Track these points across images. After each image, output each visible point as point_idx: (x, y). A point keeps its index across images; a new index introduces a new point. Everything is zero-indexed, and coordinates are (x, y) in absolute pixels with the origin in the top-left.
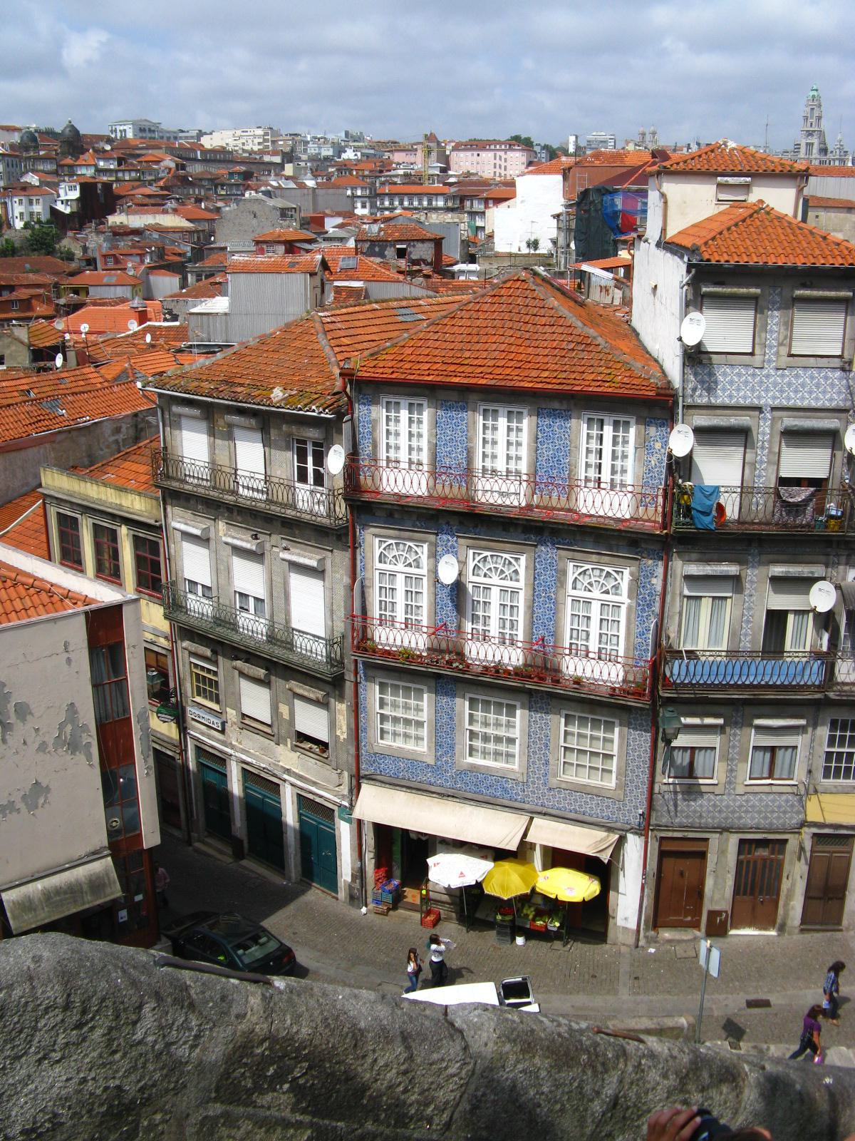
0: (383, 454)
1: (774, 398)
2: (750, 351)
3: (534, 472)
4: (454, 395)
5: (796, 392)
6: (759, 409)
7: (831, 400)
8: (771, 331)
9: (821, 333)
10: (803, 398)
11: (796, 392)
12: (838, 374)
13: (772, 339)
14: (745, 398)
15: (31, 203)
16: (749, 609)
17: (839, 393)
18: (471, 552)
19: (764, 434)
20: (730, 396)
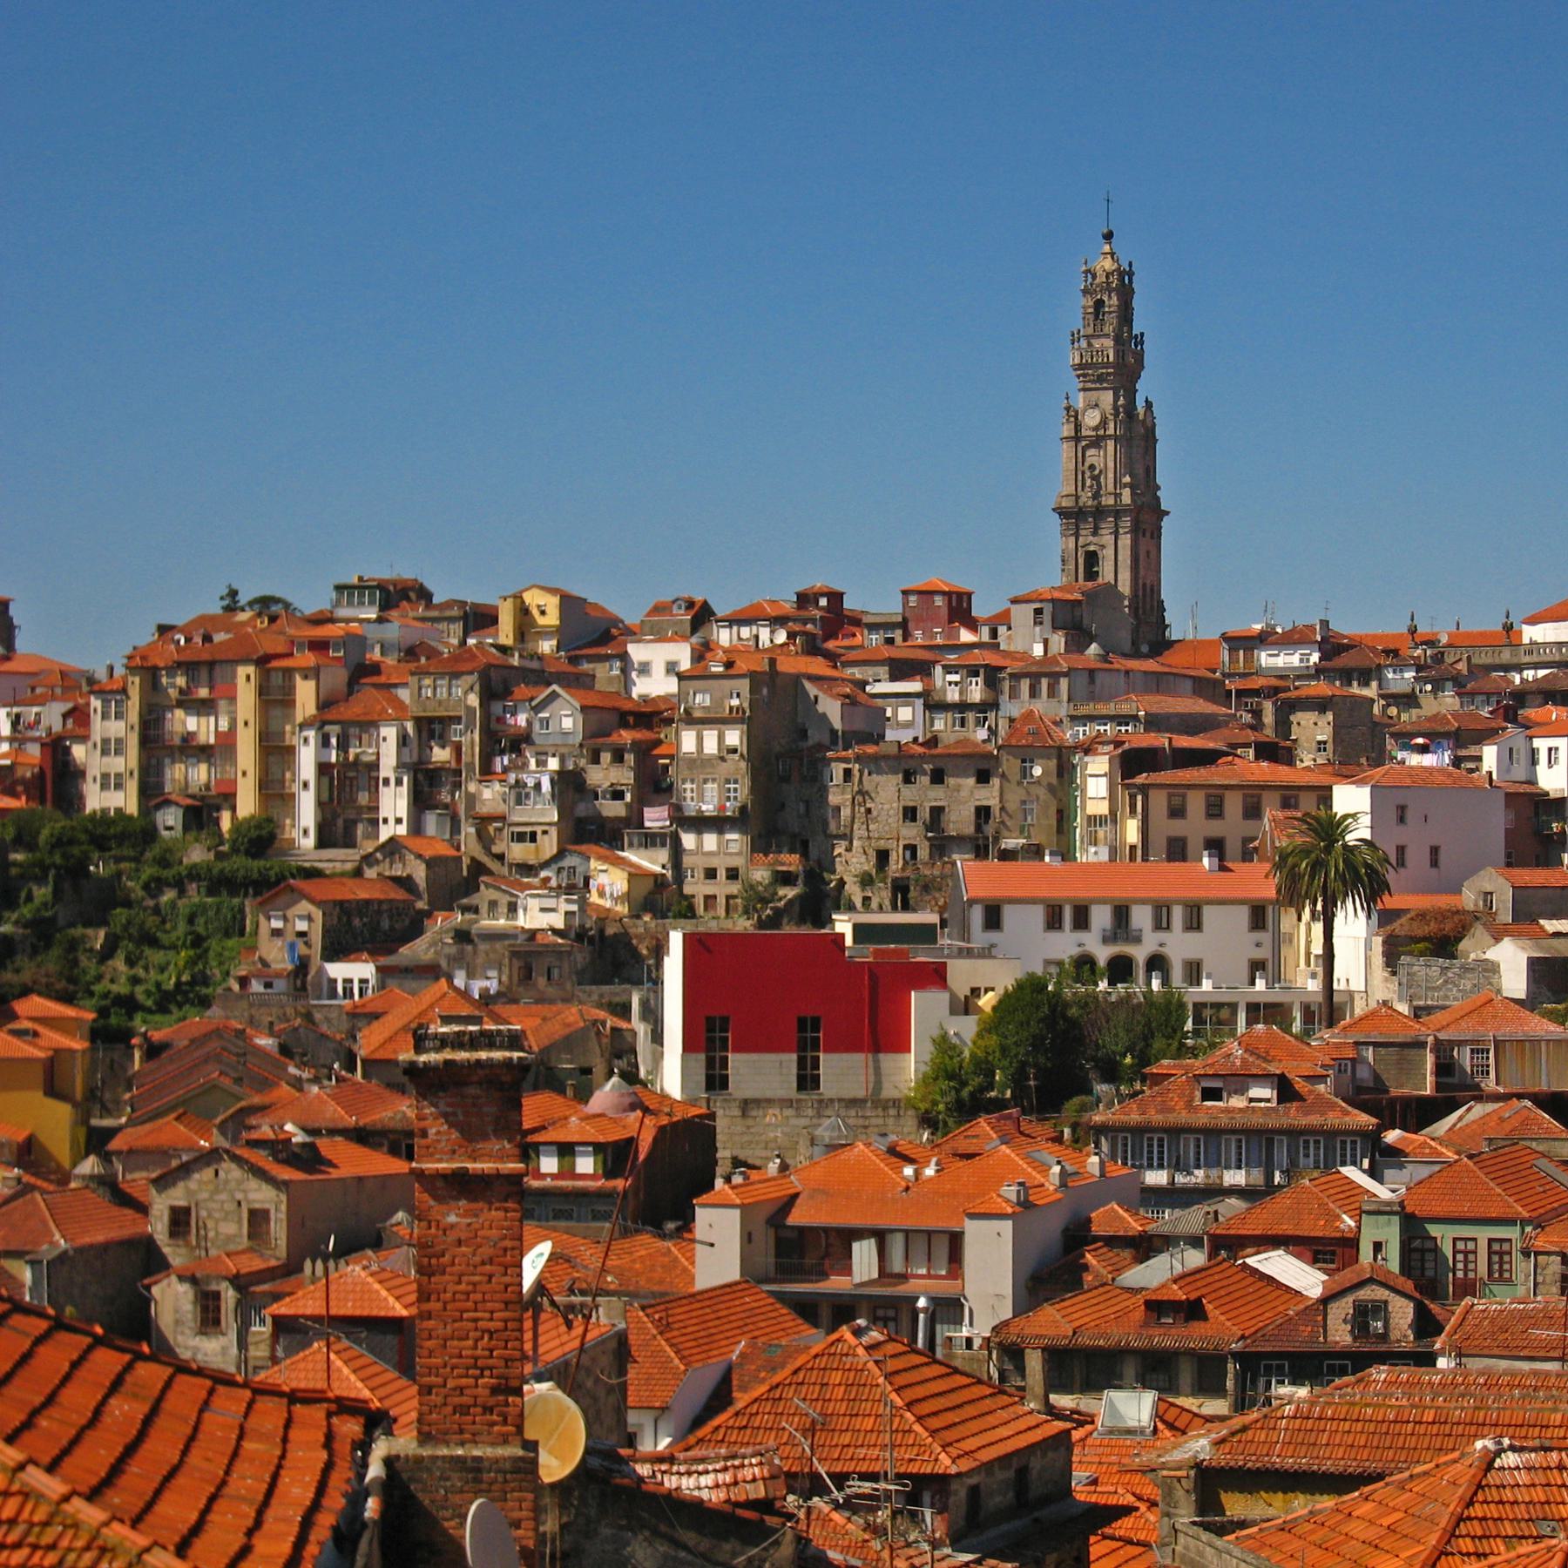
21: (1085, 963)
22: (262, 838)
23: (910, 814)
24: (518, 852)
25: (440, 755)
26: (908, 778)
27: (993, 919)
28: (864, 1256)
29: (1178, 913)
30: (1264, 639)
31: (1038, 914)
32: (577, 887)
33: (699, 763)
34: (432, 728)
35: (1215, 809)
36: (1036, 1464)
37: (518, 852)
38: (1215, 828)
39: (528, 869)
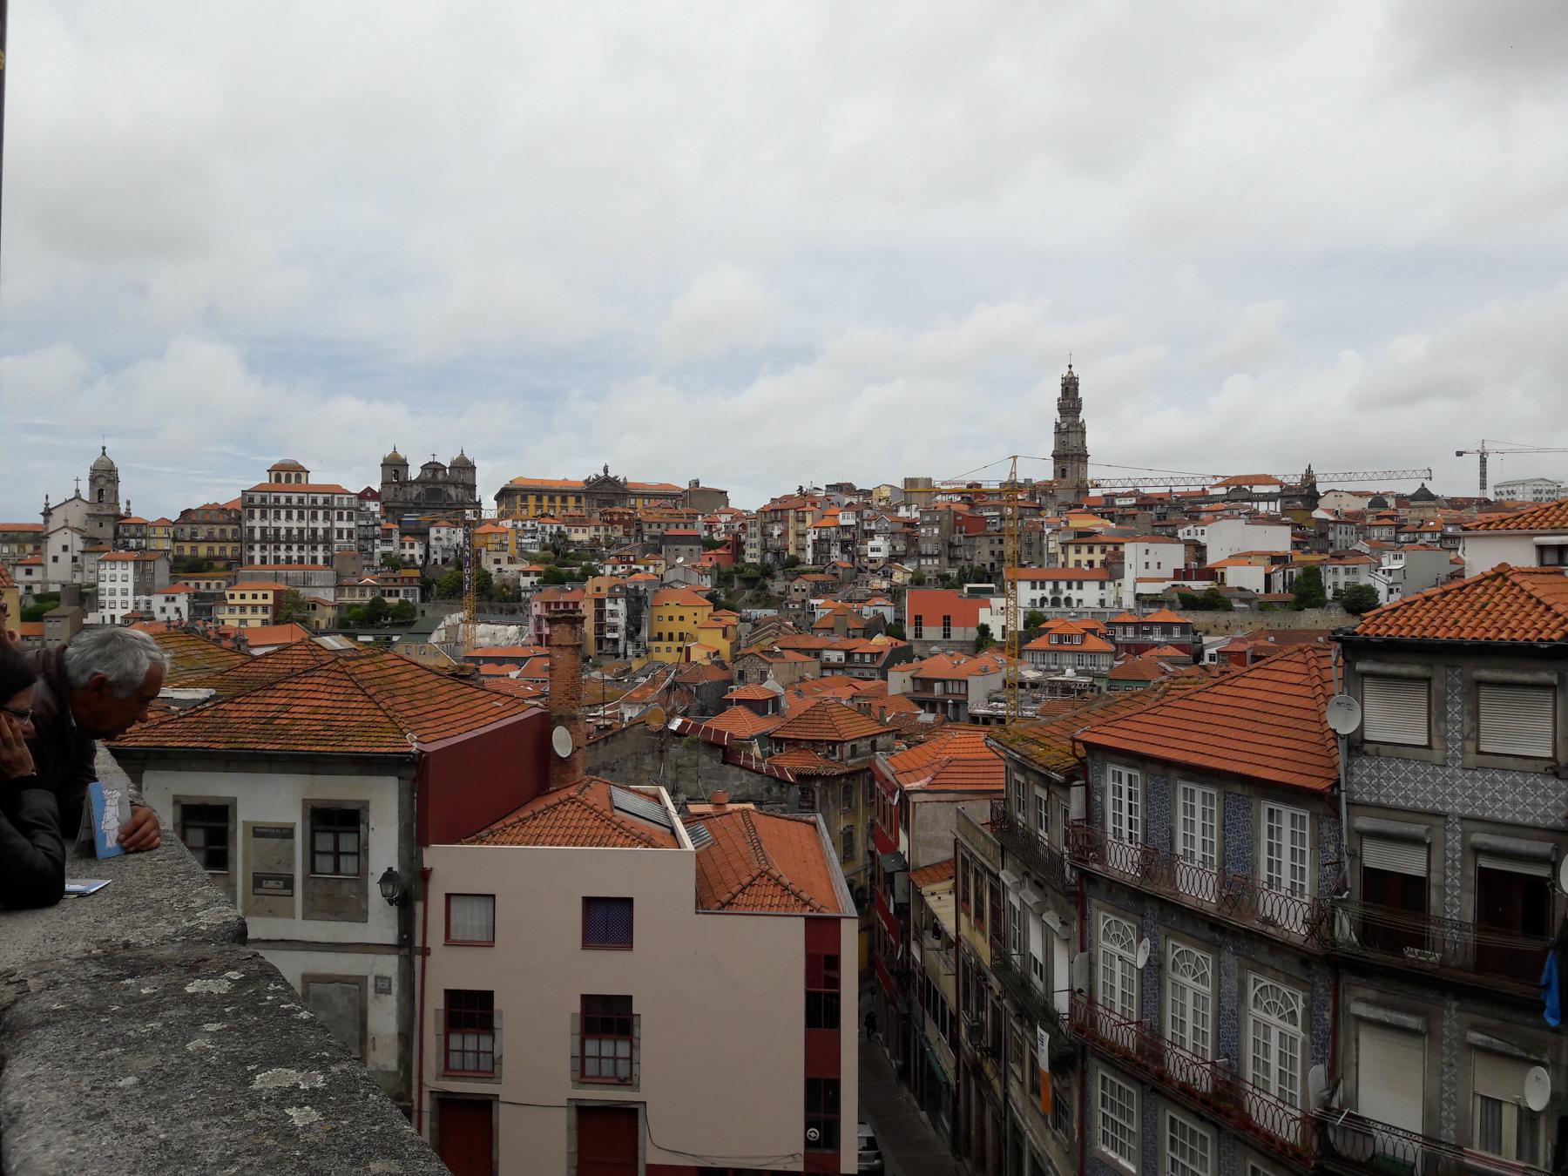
0: (1110, 825)
1: (1464, 806)
2: (1425, 743)
3: (1223, 861)
4: (1158, 769)
5: (1494, 800)
6: (1444, 816)
7: (1546, 816)
8: (1454, 722)
9: (1523, 729)
10: (1503, 810)
11: (1494, 800)
12: (1552, 782)
13: (1454, 731)
14: (1425, 801)
15: (1347, 572)
16: (1450, 1084)
17: (1557, 808)
18: (1171, 942)
19: (1454, 850)
20: (1406, 797)
21: (1044, 600)
22: (795, 561)
23: (992, 553)
24: (872, 566)
25: (848, 536)
26: (992, 542)
27: (1014, 587)
28: (938, 686)
29: (1075, 585)
30: (1116, 495)
31: (1028, 584)
32: (888, 575)
33: (926, 538)
34: (846, 528)
35: (1091, 551)
36: (880, 740)
37: (872, 566)
38: (1091, 557)
39: (873, 571)
